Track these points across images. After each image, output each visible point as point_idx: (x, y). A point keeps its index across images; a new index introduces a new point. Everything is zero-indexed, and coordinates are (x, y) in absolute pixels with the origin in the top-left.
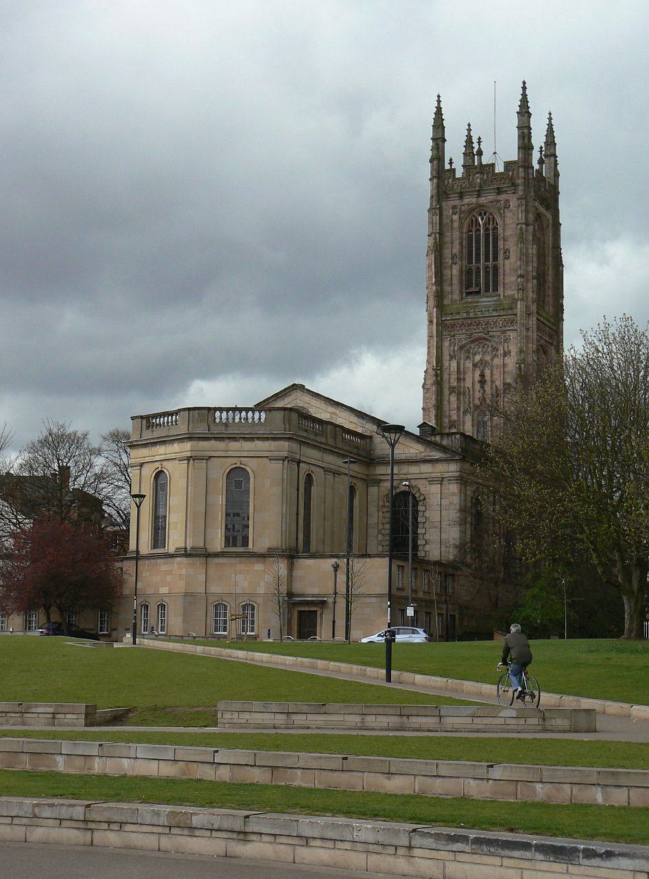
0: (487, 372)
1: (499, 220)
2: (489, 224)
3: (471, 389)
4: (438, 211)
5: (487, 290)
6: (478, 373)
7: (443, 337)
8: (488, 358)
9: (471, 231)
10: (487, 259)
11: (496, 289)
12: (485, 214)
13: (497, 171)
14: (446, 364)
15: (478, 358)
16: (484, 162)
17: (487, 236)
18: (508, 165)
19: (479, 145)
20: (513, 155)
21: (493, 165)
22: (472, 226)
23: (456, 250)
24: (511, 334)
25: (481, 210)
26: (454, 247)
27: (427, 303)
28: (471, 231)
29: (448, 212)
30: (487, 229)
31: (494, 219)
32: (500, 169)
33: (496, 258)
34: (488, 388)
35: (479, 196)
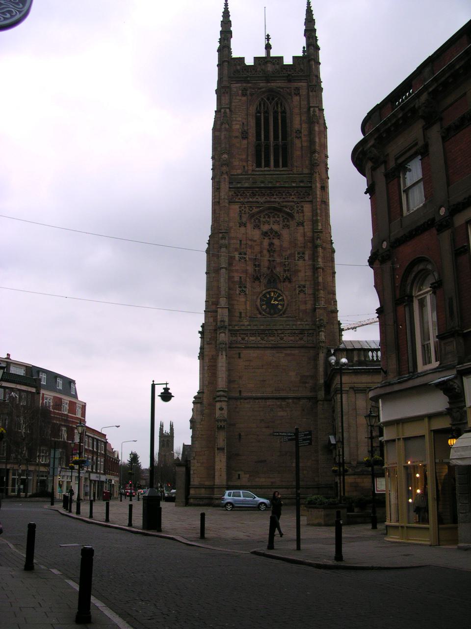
0: (276, 242)
2: (277, 108)
5: (276, 165)
6: (266, 242)
8: (276, 227)
10: (276, 137)
11: (285, 165)
12: (273, 99)
13: (285, 63)
15: (265, 228)
16: (272, 55)
19: (268, 40)
21: (281, 58)
22: (260, 109)
25: (272, 94)
30: (276, 113)
32: (288, 61)
33: (284, 137)
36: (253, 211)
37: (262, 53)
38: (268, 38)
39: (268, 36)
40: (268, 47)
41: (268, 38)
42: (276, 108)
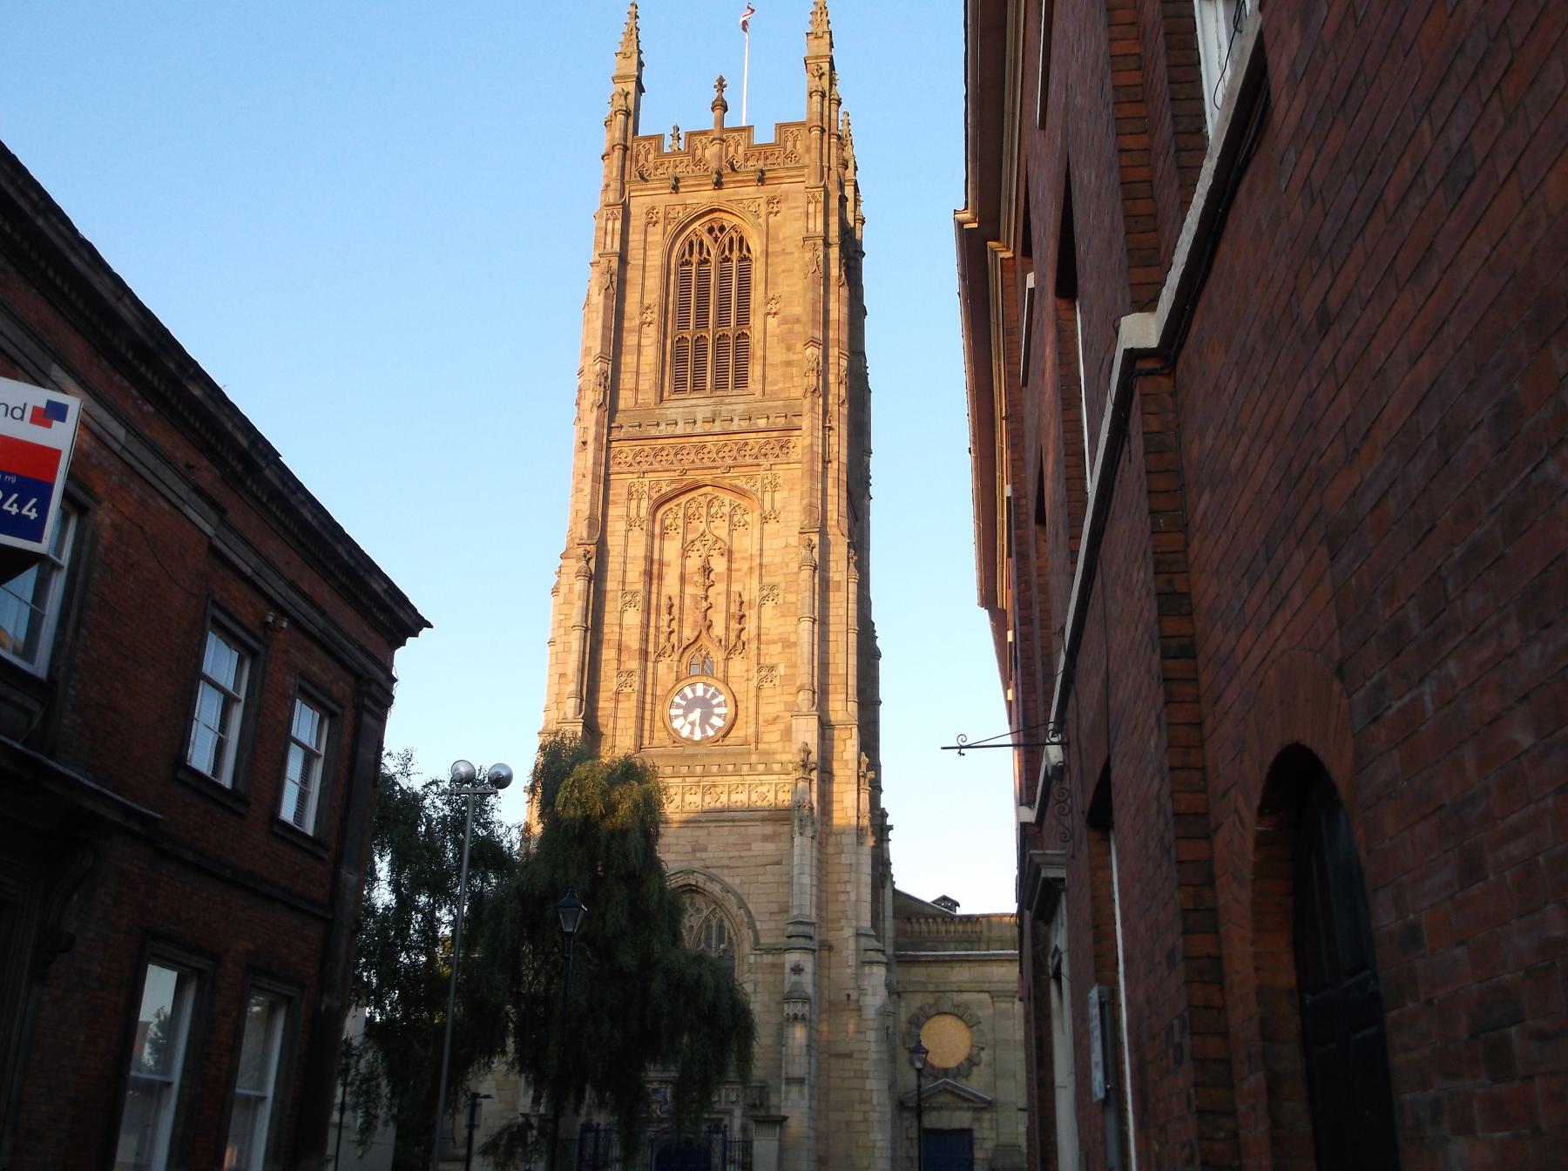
0: (719, 564)
1: (756, 244)
3: (676, 601)
4: (618, 211)
7: (612, 477)
9: (688, 263)
10: (722, 320)
11: (741, 381)
14: (614, 542)
17: (724, 277)
18: (781, 127)
20: (798, 108)
21: (748, 129)
23: (653, 296)
24: (781, 473)
26: (646, 289)
27: (578, 404)
28: (688, 263)
29: (636, 223)
31: (741, 240)
33: (744, 319)
34: (718, 593)
35: (719, 185)
36: (663, 491)
37: (707, 121)
38: (721, 85)
39: (721, 80)
40: (721, 106)
41: (721, 85)
42: (727, 252)
